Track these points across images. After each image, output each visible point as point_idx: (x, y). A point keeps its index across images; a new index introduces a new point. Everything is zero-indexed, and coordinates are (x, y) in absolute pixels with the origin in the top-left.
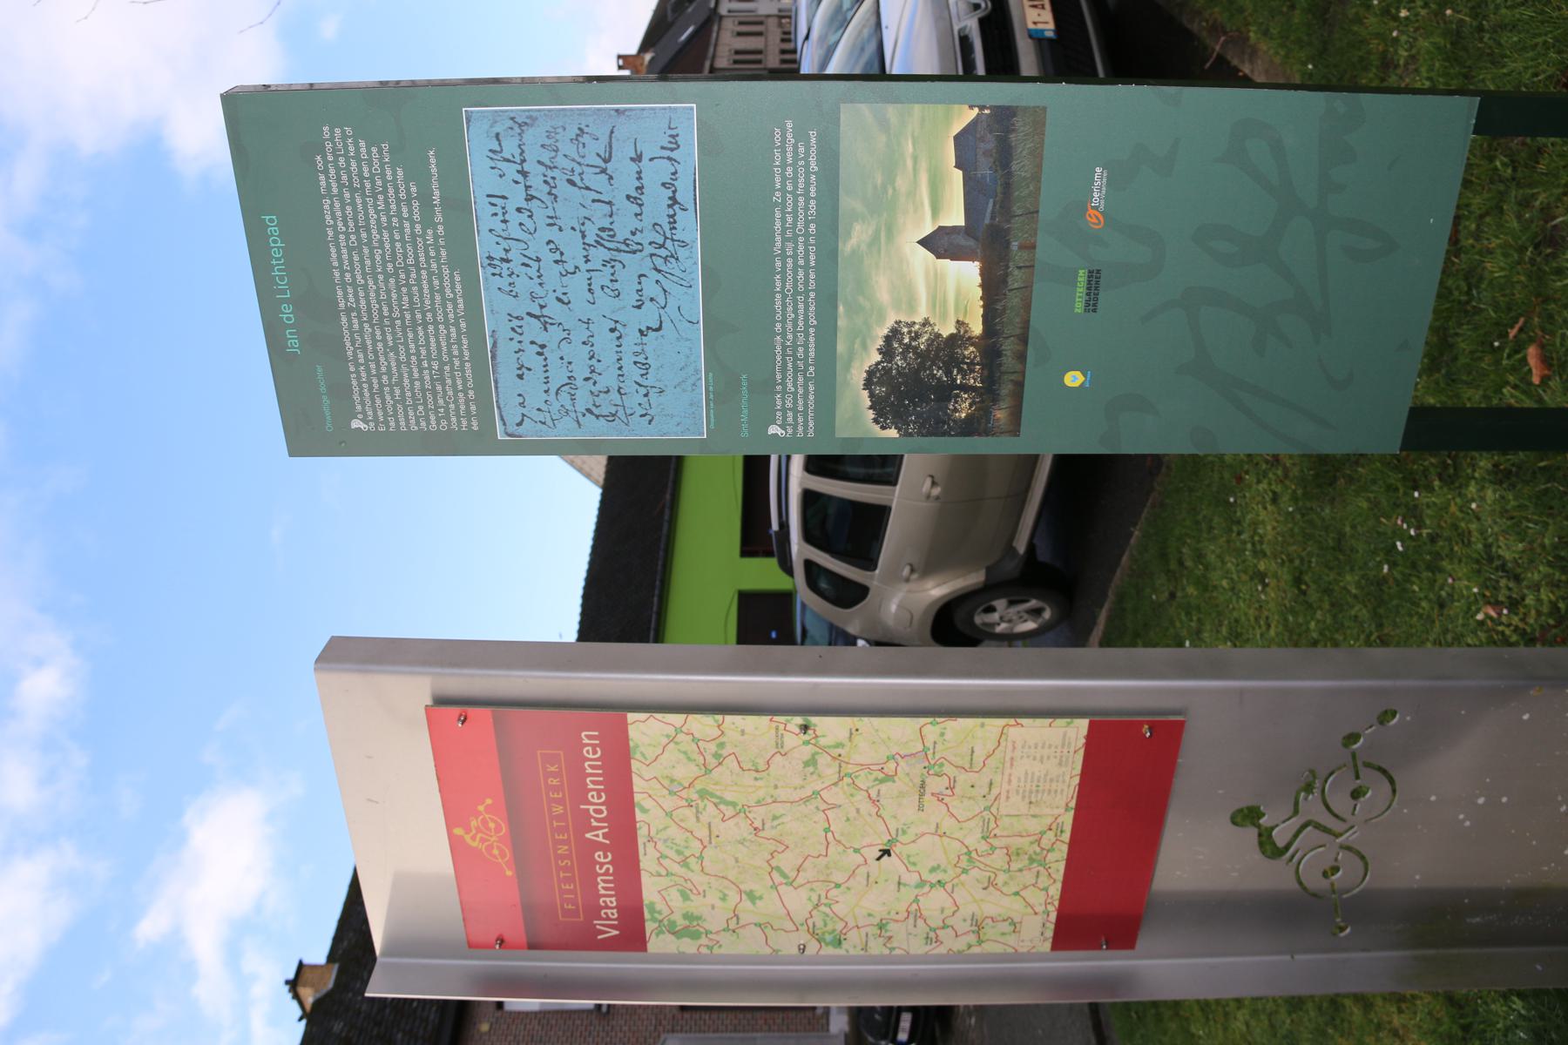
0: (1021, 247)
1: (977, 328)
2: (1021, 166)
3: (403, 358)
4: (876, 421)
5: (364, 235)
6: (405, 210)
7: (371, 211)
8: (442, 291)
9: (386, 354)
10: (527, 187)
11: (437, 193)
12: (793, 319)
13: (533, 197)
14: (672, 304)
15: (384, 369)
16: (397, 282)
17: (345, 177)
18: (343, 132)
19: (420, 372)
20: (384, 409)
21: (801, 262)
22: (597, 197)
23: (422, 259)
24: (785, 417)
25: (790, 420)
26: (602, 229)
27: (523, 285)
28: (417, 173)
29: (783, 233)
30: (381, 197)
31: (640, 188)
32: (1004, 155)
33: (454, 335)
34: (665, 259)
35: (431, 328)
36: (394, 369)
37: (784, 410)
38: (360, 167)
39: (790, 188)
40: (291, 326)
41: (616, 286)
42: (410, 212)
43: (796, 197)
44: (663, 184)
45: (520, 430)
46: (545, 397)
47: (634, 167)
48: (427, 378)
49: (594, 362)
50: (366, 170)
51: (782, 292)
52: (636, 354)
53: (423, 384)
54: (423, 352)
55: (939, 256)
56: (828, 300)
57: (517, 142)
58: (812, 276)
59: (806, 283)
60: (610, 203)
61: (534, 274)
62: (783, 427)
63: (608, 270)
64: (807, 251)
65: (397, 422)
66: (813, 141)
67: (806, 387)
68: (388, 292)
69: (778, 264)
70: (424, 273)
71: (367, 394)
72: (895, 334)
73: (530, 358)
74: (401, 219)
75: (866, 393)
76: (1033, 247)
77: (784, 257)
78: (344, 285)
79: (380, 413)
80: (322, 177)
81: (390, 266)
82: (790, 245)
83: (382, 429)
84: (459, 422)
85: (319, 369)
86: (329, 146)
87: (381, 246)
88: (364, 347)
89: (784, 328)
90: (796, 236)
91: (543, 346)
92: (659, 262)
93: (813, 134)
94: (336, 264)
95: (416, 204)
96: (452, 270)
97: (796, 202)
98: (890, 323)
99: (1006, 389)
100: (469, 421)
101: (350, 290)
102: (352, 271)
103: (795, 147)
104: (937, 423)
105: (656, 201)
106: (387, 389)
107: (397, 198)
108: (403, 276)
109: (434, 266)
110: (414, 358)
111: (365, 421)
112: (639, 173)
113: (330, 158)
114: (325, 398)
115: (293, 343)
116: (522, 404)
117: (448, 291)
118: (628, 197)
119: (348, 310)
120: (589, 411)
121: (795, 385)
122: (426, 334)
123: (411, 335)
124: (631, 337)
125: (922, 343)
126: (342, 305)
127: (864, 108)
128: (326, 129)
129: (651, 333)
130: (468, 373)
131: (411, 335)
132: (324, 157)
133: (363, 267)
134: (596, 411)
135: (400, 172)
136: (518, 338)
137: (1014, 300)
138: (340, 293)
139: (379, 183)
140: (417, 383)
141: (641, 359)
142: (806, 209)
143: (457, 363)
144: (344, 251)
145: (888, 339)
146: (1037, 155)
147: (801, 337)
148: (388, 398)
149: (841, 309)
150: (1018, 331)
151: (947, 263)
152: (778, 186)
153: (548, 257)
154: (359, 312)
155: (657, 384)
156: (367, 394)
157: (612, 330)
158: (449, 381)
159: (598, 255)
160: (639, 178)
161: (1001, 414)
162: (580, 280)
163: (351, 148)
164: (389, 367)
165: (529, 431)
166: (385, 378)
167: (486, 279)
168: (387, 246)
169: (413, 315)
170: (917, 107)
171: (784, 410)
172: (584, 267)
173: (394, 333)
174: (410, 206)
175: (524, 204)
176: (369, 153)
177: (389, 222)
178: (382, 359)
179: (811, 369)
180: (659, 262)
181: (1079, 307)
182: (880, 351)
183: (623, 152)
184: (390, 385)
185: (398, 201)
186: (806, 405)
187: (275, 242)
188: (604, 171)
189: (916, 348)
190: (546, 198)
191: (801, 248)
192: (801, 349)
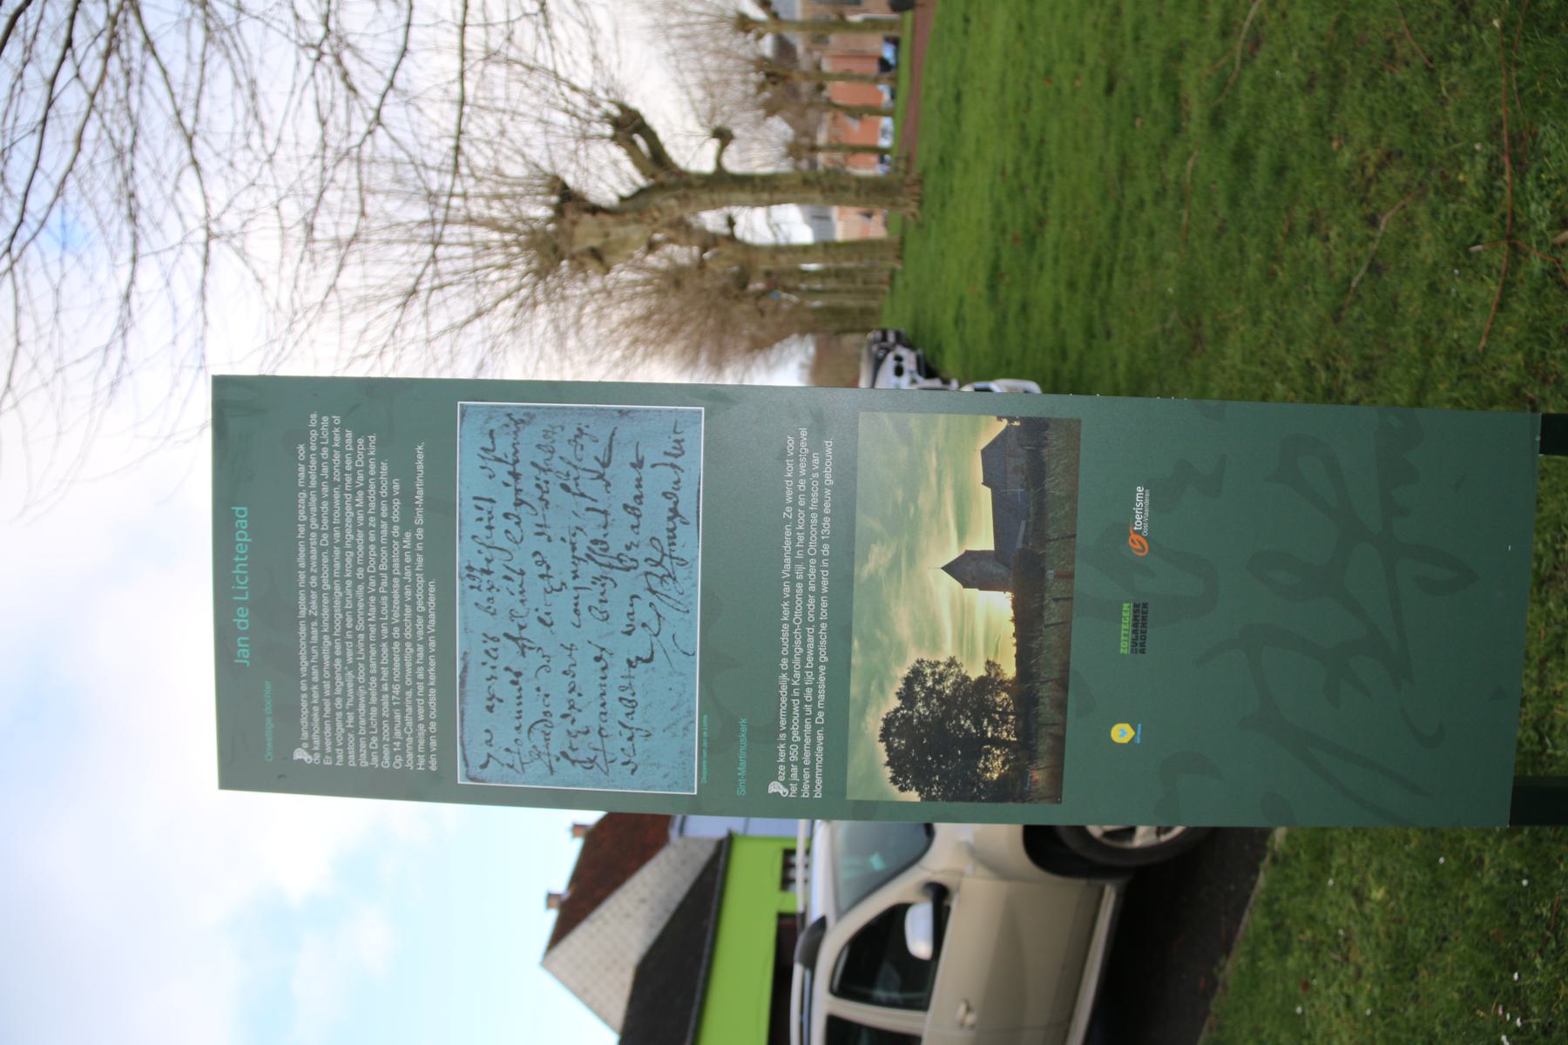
0: (1058, 576)
1: (1010, 670)
2: (1055, 486)
3: (361, 678)
4: (894, 780)
5: (337, 534)
6: (384, 509)
7: (349, 508)
8: (413, 603)
9: (343, 672)
10: (518, 491)
11: (420, 492)
12: (801, 654)
14: (665, 637)
15: (338, 691)
16: (366, 590)
17: (325, 470)
18: (331, 420)
19: (380, 694)
20: (333, 738)
21: (812, 588)
22: (592, 504)
23: (396, 565)
25: (794, 776)
26: (595, 542)
27: (503, 601)
28: (402, 469)
29: (793, 554)
30: (360, 494)
31: (639, 498)
32: (1037, 473)
33: (421, 655)
34: (662, 578)
35: (396, 645)
36: (350, 691)
37: (788, 764)
38: (343, 459)
40: (244, 633)
41: (606, 607)
42: (390, 511)
43: (808, 513)
44: (664, 494)
46: (515, 734)
47: (634, 474)
48: (386, 704)
49: (574, 695)
50: (349, 462)
51: (790, 622)
52: (623, 689)
53: (380, 712)
54: (385, 672)
55: (966, 585)
56: (841, 634)
57: (511, 440)
58: (824, 604)
60: (605, 513)
62: (786, 784)
63: (598, 588)
65: (346, 755)
66: (829, 451)
67: (813, 736)
68: (355, 600)
69: (787, 589)
70: (396, 581)
72: (916, 675)
73: (503, 687)
75: (882, 746)
76: (1071, 576)
77: (793, 580)
78: (308, 589)
79: (328, 743)
80: (302, 468)
81: (360, 571)
82: (800, 568)
83: (328, 762)
84: (416, 760)
85: (268, 685)
86: (314, 435)
87: (354, 549)
89: (791, 665)
91: (518, 674)
92: (654, 581)
94: (302, 565)
96: (427, 579)
97: (808, 519)
98: (911, 662)
99: (1044, 745)
100: (427, 759)
101: (314, 595)
102: (320, 573)
106: (339, 715)
108: (373, 583)
109: (408, 573)
110: (373, 680)
111: (311, 752)
112: (639, 480)
113: (313, 448)
114: (269, 721)
115: (244, 653)
116: (489, 742)
117: (420, 603)
119: (310, 619)
120: (564, 754)
121: (801, 734)
122: (391, 652)
123: (373, 652)
124: (618, 668)
125: (947, 687)
126: (303, 613)
127: (885, 418)
128: (314, 416)
129: (641, 665)
130: (432, 701)
131: (373, 652)
132: (308, 446)
133: (331, 572)
134: (572, 755)
136: (491, 662)
137: (1051, 638)
139: (361, 477)
140: (374, 710)
141: (627, 695)
142: (820, 527)
143: (421, 688)
144: (314, 551)
145: (909, 682)
146: (1073, 470)
148: (339, 725)
149: (856, 644)
150: (1056, 675)
151: (974, 593)
153: (533, 570)
154: (320, 622)
157: (598, 659)
159: (589, 570)
160: (639, 486)
161: (1038, 776)
162: (566, 597)
163: (337, 438)
164: (345, 689)
165: (494, 777)
166: (339, 701)
167: (463, 592)
168: (361, 548)
170: (941, 418)
171: (788, 764)
172: (571, 584)
173: (355, 649)
174: (390, 505)
175: (512, 509)
176: (355, 444)
177: (366, 521)
178: (338, 678)
179: (821, 715)
180: (654, 581)
181: (1125, 647)
182: (899, 695)
184: (344, 711)
186: (813, 758)
187: (242, 536)
188: (601, 476)
189: (941, 693)
191: (813, 572)
192: (809, 691)
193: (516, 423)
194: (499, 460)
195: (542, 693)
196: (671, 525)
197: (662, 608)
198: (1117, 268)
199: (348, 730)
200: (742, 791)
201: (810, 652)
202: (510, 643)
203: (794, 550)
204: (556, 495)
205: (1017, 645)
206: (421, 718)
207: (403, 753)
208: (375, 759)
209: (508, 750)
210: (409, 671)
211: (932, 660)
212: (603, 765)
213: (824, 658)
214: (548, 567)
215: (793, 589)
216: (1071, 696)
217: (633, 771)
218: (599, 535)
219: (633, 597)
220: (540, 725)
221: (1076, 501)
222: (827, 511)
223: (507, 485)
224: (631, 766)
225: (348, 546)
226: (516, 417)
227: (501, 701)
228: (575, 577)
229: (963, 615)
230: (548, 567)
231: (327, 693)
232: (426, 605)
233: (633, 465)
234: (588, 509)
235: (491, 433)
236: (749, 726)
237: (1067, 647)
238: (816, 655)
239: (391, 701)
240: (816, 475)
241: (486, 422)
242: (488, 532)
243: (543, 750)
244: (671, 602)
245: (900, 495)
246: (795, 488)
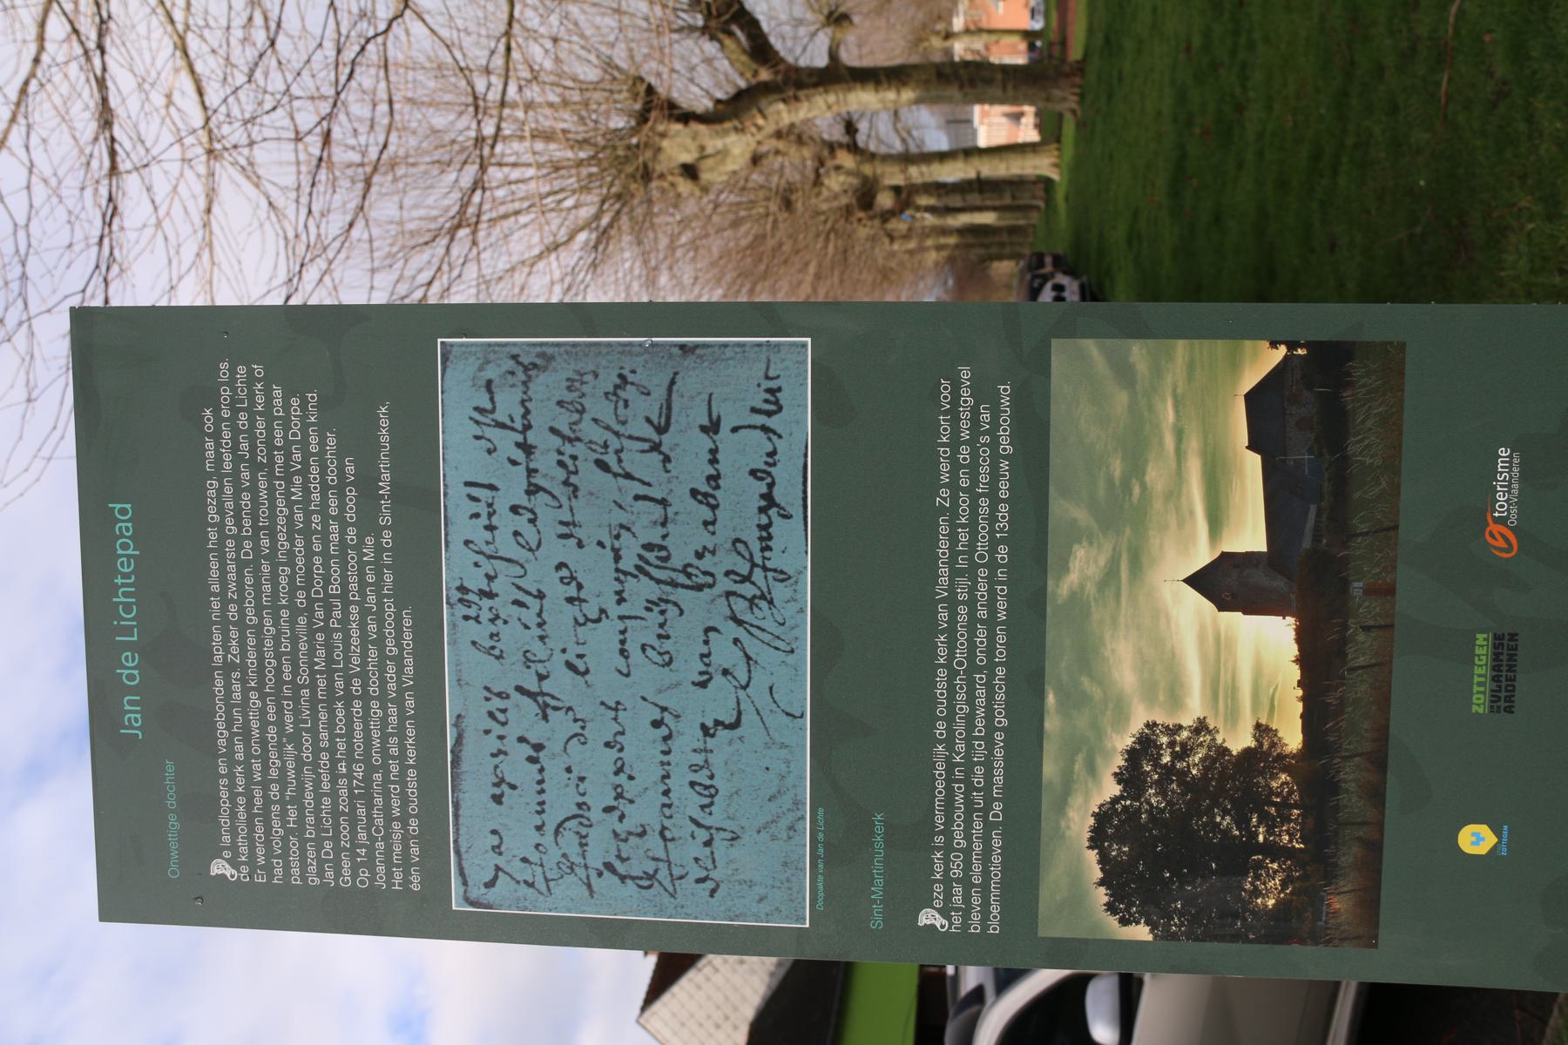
0: (1369, 591)
1: (1292, 738)
2: (1364, 448)
3: (307, 755)
4: (1111, 908)
5: (265, 542)
6: (333, 503)
7: (281, 503)
8: (380, 642)
9: (280, 746)
10: (531, 472)
11: (386, 476)
12: (966, 712)
15: (274, 773)
16: (310, 624)
17: (245, 445)
18: (250, 371)
20: (268, 843)
21: (983, 613)
23: (354, 587)
24: (948, 895)
25: (958, 900)
26: (649, 547)
27: (513, 638)
28: (360, 445)
30: (297, 480)
32: (1334, 428)
33: (393, 720)
34: (751, 601)
35: (357, 705)
36: (291, 774)
37: (947, 881)
39: (964, 482)
41: (667, 645)
42: (342, 507)
44: (753, 473)
45: (491, 895)
46: (536, 837)
47: (706, 442)
48: (344, 792)
49: (622, 778)
51: (948, 666)
52: (695, 768)
53: (335, 804)
55: (1222, 606)
56: (1028, 683)
57: (518, 394)
58: (1001, 638)
59: (991, 651)
60: (663, 502)
61: (532, 619)
62: (944, 912)
63: (654, 617)
64: (992, 593)
65: (287, 867)
66: (1005, 401)
67: (986, 840)
68: (294, 640)
69: (943, 615)
70: (354, 609)
71: (242, 816)
72: (1145, 746)
73: (517, 767)
74: (326, 518)
75: (1093, 856)
76: (1390, 591)
78: (225, 624)
79: (260, 851)
80: (210, 444)
81: (301, 595)
82: (963, 582)
84: (389, 875)
85: (170, 768)
86: (226, 393)
87: (291, 563)
88: (246, 734)
90: (973, 567)
91: (538, 747)
92: (740, 606)
93: (1005, 390)
94: (216, 588)
95: (351, 493)
96: (400, 607)
97: (974, 507)
98: (1137, 725)
99: (1348, 855)
100: (407, 874)
101: (234, 634)
102: (241, 601)
103: (975, 412)
104: (1222, 916)
106: (276, 808)
108: (320, 614)
109: (372, 598)
110: (325, 757)
111: (234, 863)
112: (714, 451)
113: (226, 414)
114: (173, 819)
115: (133, 718)
117: (390, 643)
118: (694, 493)
119: (228, 668)
121: (968, 837)
122: (349, 717)
124: (688, 738)
126: (218, 658)
127: (1091, 347)
128: (224, 366)
129: (722, 734)
130: (412, 787)
132: (217, 411)
133: (258, 598)
136: (498, 730)
137: (1360, 688)
138: (217, 637)
139: (297, 456)
140: (326, 801)
141: (702, 777)
142: (992, 519)
143: (394, 769)
144: (232, 567)
145: (1133, 756)
146: (1392, 423)
147: (980, 747)
148: (276, 824)
149: (1051, 699)
151: (1237, 617)
152: (945, 479)
153: (557, 592)
154: (244, 673)
155: (727, 824)
156: (242, 816)
157: (656, 724)
158: (379, 801)
159: (641, 590)
160: (713, 462)
161: (1340, 904)
162: (610, 628)
163: (260, 399)
164: (283, 770)
165: (506, 899)
166: (275, 788)
167: (453, 626)
168: (300, 562)
169: (331, 681)
170: (1181, 346)
172: (614, 611)
173: (296, 712)
174: (341, 496)
175: (523, 500)
176: (286, 406)
178: (273, 755)
179: (997, 807)
180: (740, 606)
181: (1480, 703)
182: (1119, 777)
183: (689, 415)
184: (283, 803)
185: (325, 487)
186: (986, 873)
187: (125, 546)
188: (656, 447)
189: (1184, 773)
190: (558, 490)
191: (982, 589)
192: (979, 771)
193: (526, 369)
194: (503, 426)
195: (574, 776)
196: (764, 520)
198: (1345, 159)
199: (289, 832)
200: (877, 922)
201: (981, 712)
202: (526, 700)
203: (954, 555)
204: (589, 476)
205: (1304, 699)
206: (396, 813)
207: (370, 864)
208: (330, 874)
209: (525, 860)
210: (376, 743)
211: (1171, 722)
212: (667, 883)
213: (1001, 720)
214: (580, 587)
215: (953, 615)
216: (1389, 775)
217: (713, 892)
219: (708, 630)
220: (573, 824)
223: (514, 463)
224: (710, 885)
225: (282, 559)
226: (526, 360)
227: (513, 787)
228: (621, 601)
229: (1218, 653)
230: (580, 587)
231: (258, 777)
232: (399, 645)
233: (704, 429)
234: (637, 498)
235: (489, 385)
236: (887, 824)
237: (1383, 701)
238: (990, 715)
239: (350, 789)
240: (985, 439)
241: (481, 369)
242: (488, 535)
243: (578, 860)
244: (766, 637)
245: (1117, 468)
246: (953, 460)
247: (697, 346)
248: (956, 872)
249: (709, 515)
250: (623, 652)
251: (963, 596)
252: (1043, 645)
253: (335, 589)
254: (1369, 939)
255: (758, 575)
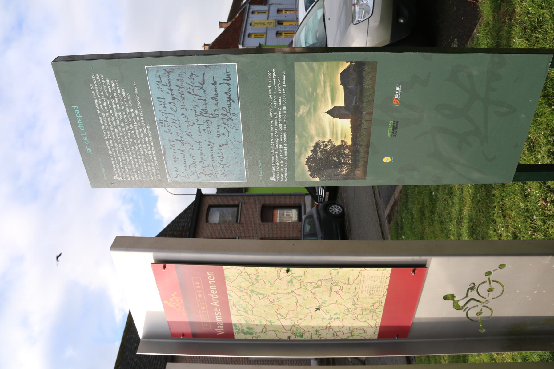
0: (367, 114)
1: (349, 142)
2: (367, 84)
3: (130, 155)
4: (311, 175)
5: (112, 113)
6: (126, 103)
7: (113, 104)
8: (143, 132)
9: (124, 154)
10: (172, 95)
11: (138, 97)
12: (278, 140)
13: (175, 98)
15: (124, 159)
16: (126, 129)
17: (102, 92)
18: (100, 76)
19: (138, 159)
20: (125, 172)
21: (281, 120)
22: (200, 98)
24: (276, 174)
25: (278, 175)
26: (203, 110)
27: (173, 129)
32: (360, 80)
33: (149, 147)
34: (228, 120)
35: (140, 145)
36: (128, 159)
37: (276, 172)
38: (107, 88)
39: (275, 93)
40: (87, 145)
41: (209, 129)
42: (128, 104)
44: (225, 93)
45: (176, 179)
46: (185, 168)
47: (214, 87)
48: (140, 162)
49: (202, 156)
50: (110, 89)
51: (273, 131)
52: (218, 153)
55: (334, 117)
58: (285, 125)
60: (205, 100)
61: (178, 126)
62: (276, 177)
65: (130, 176)
66: (284, 76)
67: (284, 164)
68: (123, 132)
69: (272, 121)
71: (118, 167)
73: (178, 155)
74: (125, 107)
75: (307, 166)
76: (372, 113)
77: (273, 118)
78: (106, 130)
80: (93, 92)
81: (122, 124)
82: (276, 115)
87: (119, 117)
88: (116, 151)
89: (274, 144)
91: (183, 151)
92: (225, 121)
93: (284, 73)
94: (102, 123)
97: (278, 99)
98: (316, 141)
99: (361, 164)
101: (108, 132)
102: (108, 125)
103: (277, 78)
105: (223, 99)
106: (125, 166)
107: (123, 99)
110: (135, 155)
112: (216, 89)
113: (96, 85)
115: (89, 150)
116: (177, 171)
117: (145, 132)
118: (212, 98)
119: (109, 139)
121: (280, 163)
122: (138, 147)
123: (133, 147)
124: (216, 148)
126: (106, 137)
127: (304, 63)
128: (93, 75)
129: (223, 146)
130: (155, 160)
131: (133, 147)
132: (93, 85)
133: (112, 125)
135: (123, 90)
136: (173, 148)
137: (364, 133)
138: (105, 133)
139: (115, 94)
140: (137, 164)
141: (220, 155)
142: (282, 101)
144: (105, 118)
145: (315, 147)
146: (374, 79)
147: (281, 147)
148: (126, 169)
149: (296, 137)
150: (365, 144)
151: (337, 120)
152: (270, 93)
153: (182, 120)
154: (112, 139)
156: (118, 167)
157: (209, 145)
158: (148, 163)
160: (216, 91)
163: (103, 81)
166: (124, 162)
167: (159, 128)
168: (121, 116)
170: (325, 63)
171: (276, 172)
172: (196, 123)
173: (126, 147)
175: (172, 101)
176: (110, 83)
178: (123, 156)
179: (286, 158)
180: (225, 121)
181: (389, 134)
182: (312, 151)
185: (123, 100)
188: (202, 88)
189: (326, 150)
190: (180, 99)
191: (280, 115)
192: (281, 151)
196: (229, 103)
197: (228, 129)
201: (281, 140)
204: (186, 95)
208: (140, 177)
210: (146, 152)
216: (370, 149)
218: (204, 107)
219: (218, 126)
221: (374, 89)
222: (284, 95)
233: (213, 84)
235: (159, 76)
237: (369, 135)
238: (283, 140)
242: (164, 109)
245: (310, 90)
247: (209, 66)
248: (277, 170)
249: (216, 102)
250: (199, 131)
251: (276, 117)
252: (294, 126)
253: (130, 121)
254: (365, 179)
255: (229, 114)
